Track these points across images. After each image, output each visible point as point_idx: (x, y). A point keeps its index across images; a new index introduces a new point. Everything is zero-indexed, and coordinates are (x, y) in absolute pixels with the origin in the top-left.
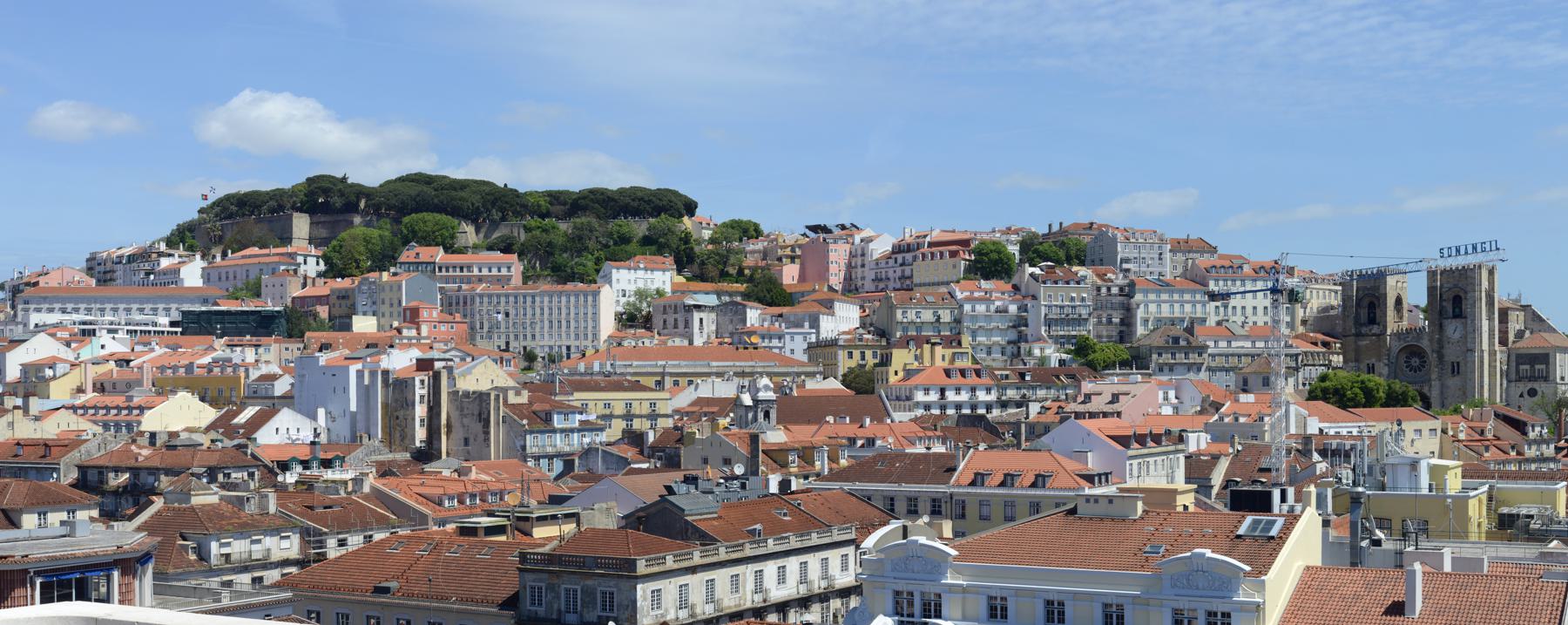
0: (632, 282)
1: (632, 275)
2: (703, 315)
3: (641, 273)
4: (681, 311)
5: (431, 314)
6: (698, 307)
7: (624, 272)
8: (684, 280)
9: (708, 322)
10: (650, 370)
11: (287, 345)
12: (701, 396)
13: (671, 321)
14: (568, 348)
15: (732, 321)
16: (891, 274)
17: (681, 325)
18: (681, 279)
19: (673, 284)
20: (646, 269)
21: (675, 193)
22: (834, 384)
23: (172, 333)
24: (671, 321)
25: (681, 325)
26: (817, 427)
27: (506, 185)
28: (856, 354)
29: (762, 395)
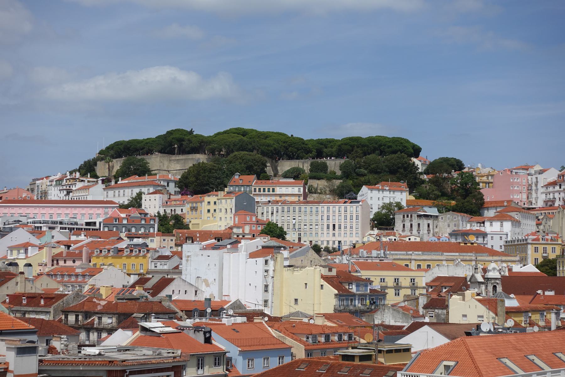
0: (381, 199)
1: (381, 195)
2: (430, 222)
3: (387, 194)
4: (415, 219)
5: (251, 219)
6: (427, 216)
7: (375, 193)
8: (414, 198)
9: (433, 227)
10: (402, 257)
11: (164, 238)
12: (439, 275)
13: (408, 224)
14: (340, 242)
15: (449, 226)
16: (557, 195)
17: (415, 228)
18: (412, 198)
19: (407, 200)
20: (390, 190)
21: (407, 141)
22: (531, 268)
23: (87, 229)
24: (408, 224)
25: (415, 228)
26: (532, 297)
27: (292, 136)
28: (541, 248)
29: (490, 275)
